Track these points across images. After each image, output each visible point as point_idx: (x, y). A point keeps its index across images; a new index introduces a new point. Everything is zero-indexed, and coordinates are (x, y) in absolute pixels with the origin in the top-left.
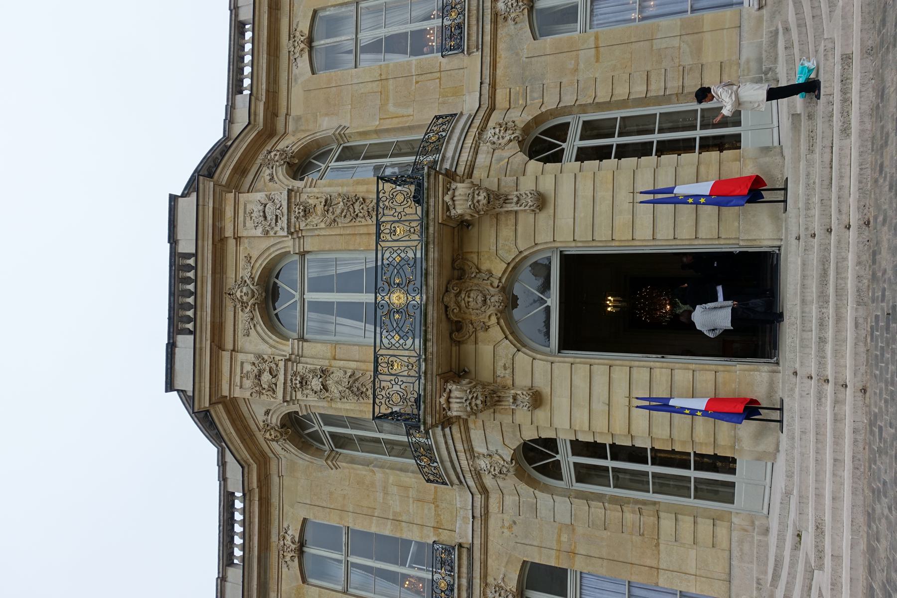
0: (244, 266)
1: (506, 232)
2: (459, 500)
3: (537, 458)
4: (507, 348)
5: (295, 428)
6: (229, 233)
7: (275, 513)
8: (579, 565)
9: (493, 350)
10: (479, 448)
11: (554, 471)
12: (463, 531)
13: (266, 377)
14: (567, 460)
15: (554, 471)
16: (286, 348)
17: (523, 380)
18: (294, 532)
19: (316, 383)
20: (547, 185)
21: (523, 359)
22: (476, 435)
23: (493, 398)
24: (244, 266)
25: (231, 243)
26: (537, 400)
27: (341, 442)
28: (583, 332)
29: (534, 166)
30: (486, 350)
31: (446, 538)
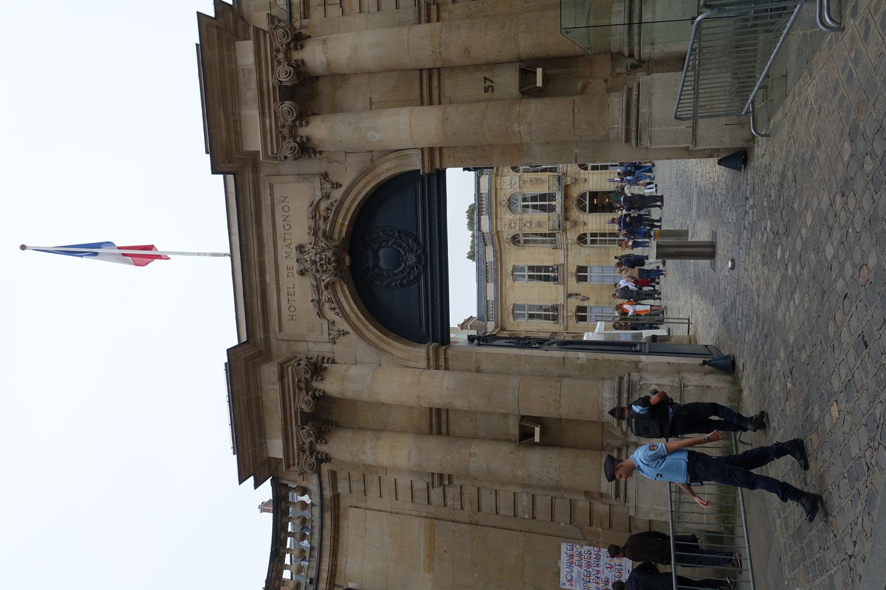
0: (503, 196)
1: (577, 187)
2: (560, 253)
3: (582, 239)
4: (577, 213)
5: (515, 240)
6: (498, 187)
7: (504, 265)
8: (591, 264)
9: (575, 213)
10: (569, 237)
11: (585, 242)
12: (561, 260)
13: (513, 225)
14: (589, 238)
15: (585, 242)
16: (518, 217)
17: (581, 220)
18: (510, 269)
19: (528, 225)
20: (586, 176)
21: (581, 215)
22: (569, 234)
23: (575, 224)
24: (503, 196)
25: (499, 191)
26: (585, 224)
27: (526, 242)
28: (594, 209)
29: (582, 171)
30: (573, 214)
31: (556, 263)
